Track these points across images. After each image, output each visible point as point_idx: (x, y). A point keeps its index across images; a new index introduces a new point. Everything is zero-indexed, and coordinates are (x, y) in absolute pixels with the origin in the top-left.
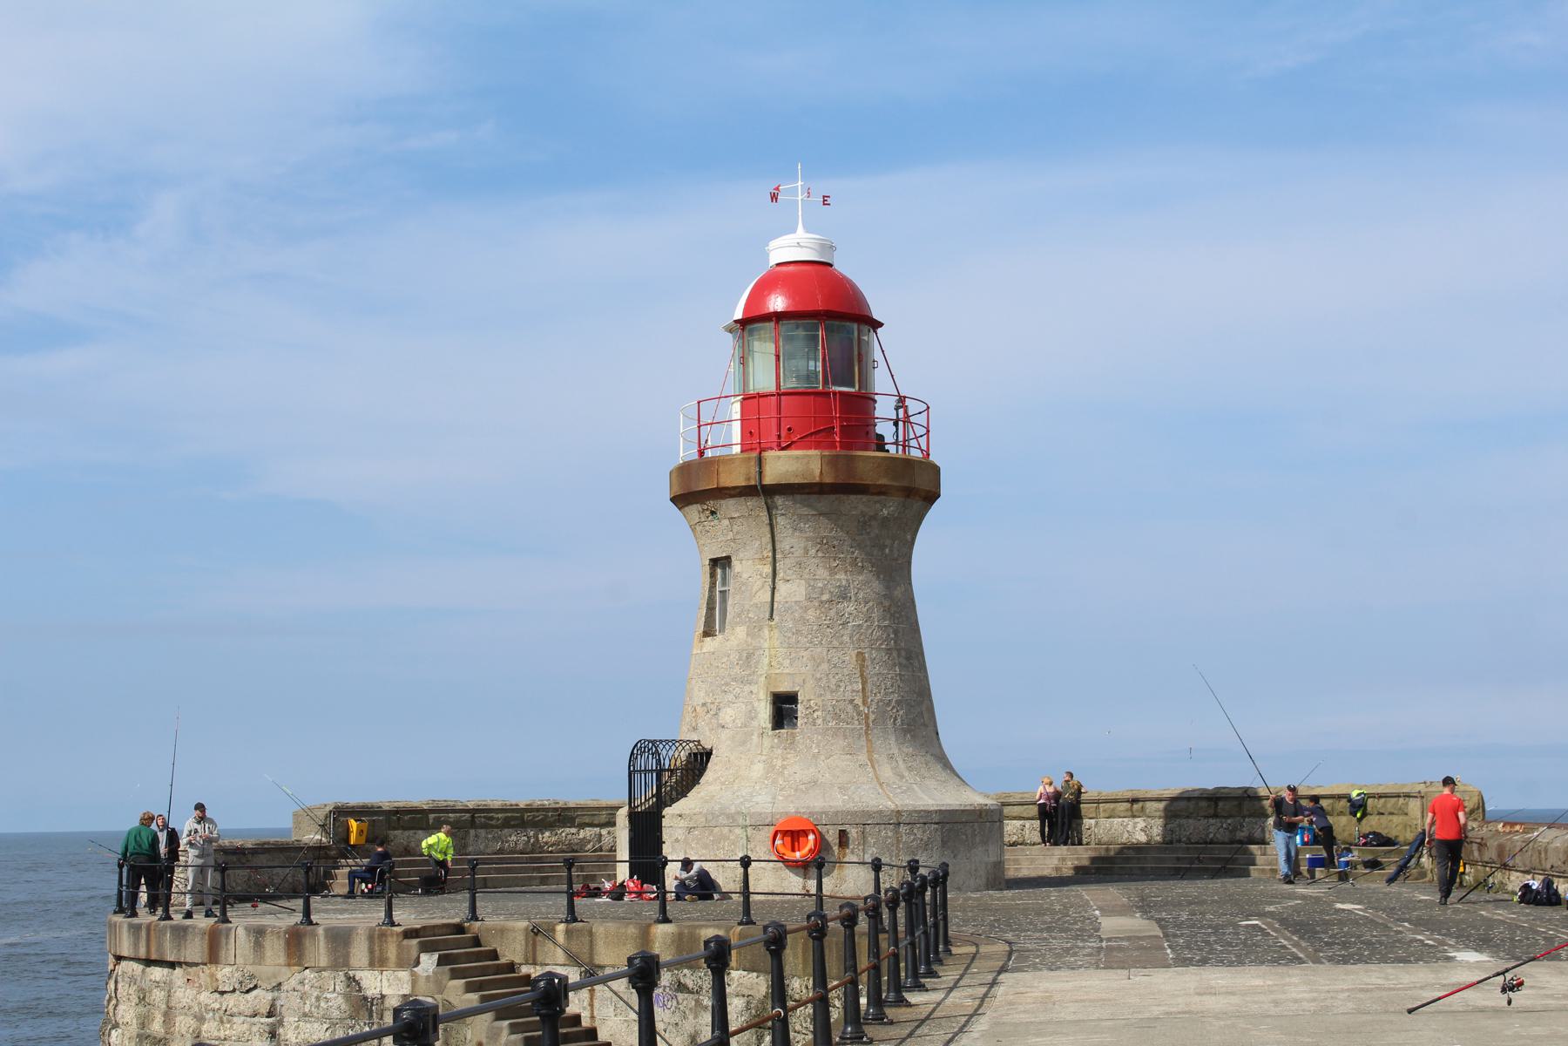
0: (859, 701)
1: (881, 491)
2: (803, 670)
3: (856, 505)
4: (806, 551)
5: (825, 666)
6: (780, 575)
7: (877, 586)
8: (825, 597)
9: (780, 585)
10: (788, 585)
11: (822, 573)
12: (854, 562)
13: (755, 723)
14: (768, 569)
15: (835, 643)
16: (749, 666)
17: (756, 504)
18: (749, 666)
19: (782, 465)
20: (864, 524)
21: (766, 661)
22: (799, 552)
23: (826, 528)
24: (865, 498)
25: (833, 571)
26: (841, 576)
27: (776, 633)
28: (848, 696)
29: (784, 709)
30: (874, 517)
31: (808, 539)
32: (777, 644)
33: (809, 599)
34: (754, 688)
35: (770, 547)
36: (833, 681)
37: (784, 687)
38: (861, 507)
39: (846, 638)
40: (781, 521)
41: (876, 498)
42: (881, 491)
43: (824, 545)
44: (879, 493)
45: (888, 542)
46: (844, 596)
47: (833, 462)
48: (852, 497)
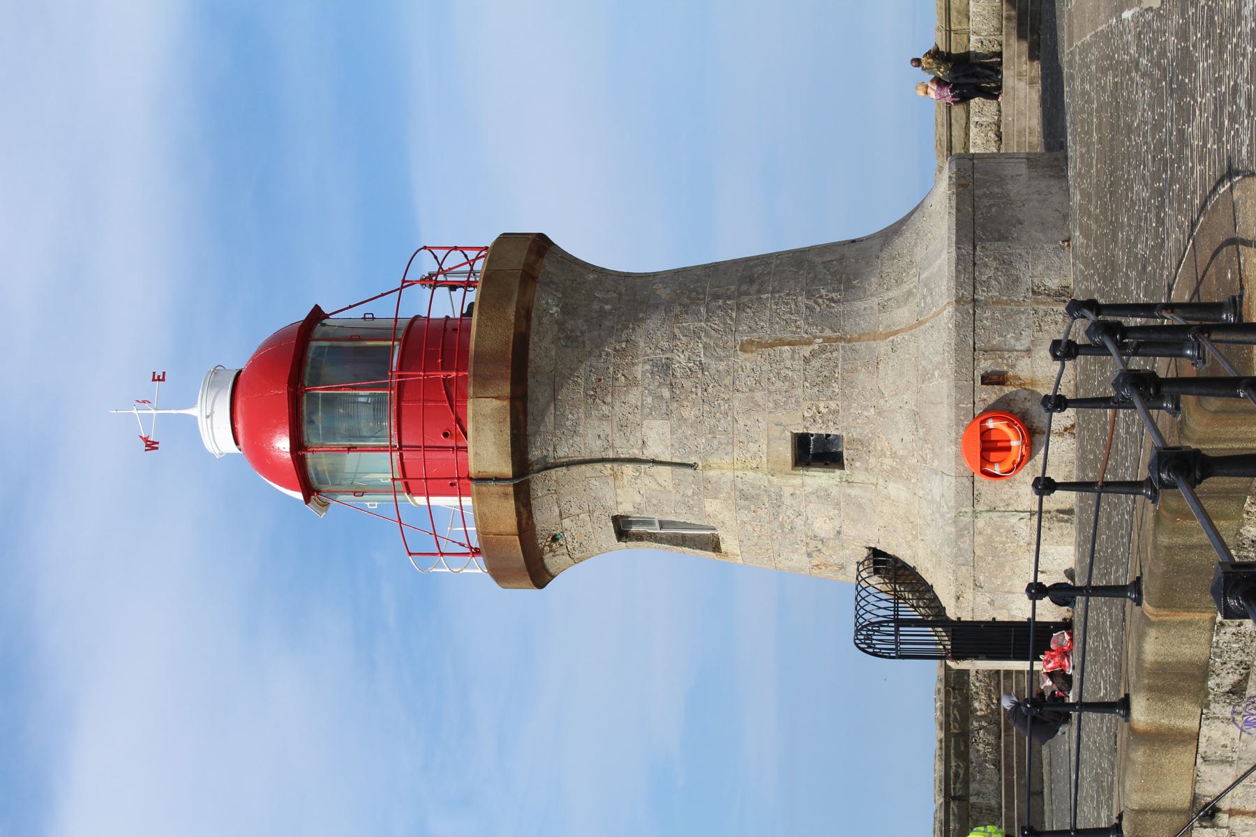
2: (763, 425)
5: (758, 395)
8: (666, 393)
10: (649, 443)
13: (835, 492)
16: (758, 497)
18: (758, 497)
21: (751, 474)
22: (606, 428)
23: (573, 392)
24: (534, 338)
29: (815, 452)
32: (728, 459)
33: (668, 415)
34: (787, 491)
36: (779, 384)
40: (564, 452)
48: (532, 355)
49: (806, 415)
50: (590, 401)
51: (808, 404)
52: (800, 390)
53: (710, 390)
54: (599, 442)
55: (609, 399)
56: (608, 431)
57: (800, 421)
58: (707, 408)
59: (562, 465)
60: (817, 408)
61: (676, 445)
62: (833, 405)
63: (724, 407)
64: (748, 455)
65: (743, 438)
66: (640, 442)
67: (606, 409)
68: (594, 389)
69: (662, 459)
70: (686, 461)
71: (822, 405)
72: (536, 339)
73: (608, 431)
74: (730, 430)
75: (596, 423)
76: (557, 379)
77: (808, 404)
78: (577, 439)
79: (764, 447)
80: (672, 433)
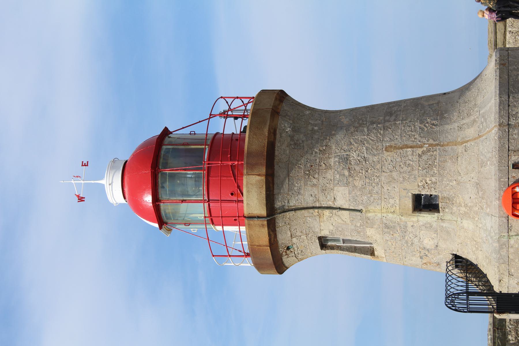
0: (420, 151)
1: (273, 132)
2: (397, 190)
3: (282, 150)
4: (314, 185)
5: (395, 174)
6: (331, 204)
7: (339, 136)
8: (346, 173)
9: (338, 204)
10: (338, 198)
11: (329, 175)
12: (323, 152)
14: (327, 212)
15: (378, 166)
17: (281, 221)
19: (253, 202)
20: (296, 145)
21: (390, 215)
22: (315, 191)
23: (298, 172)
24: (278, 144)
25: (328, 167)
26: (332, 161)
27: (371, 208)
28: (416, 158)
30: (292, 137)
31: (306, 185)
32: (378, 207)
33: (347, 184)
35: (311, 211)
37: (409, 203)
38: (283, 147)
39: (375, 159)
41: (278, 136)
42: (273, 132)
43: (311, 171)
44: (275, 134)
45: (310, 128)
46: (346, 160)
47: (251, 167)
50: (307, 177)
53: (369, 171)
54: (311, 198)
55: (316, 176)
56: (316, 192)
58: (367, 180)
59: (292, 210)
61: (352, 200)
63: (377, 180)
64: (389, 205)
65: (386, 196)
66: (333, 198)
67: (315, 181)
68: (309, 171)
69: (344, 207)
70: (357, 208)
72: (279, 145)
73: (316, 192)
74: (380, 192)
75: (310, 188)
76: (290, 165)
78: (300, 196)
79: (397, 201)
80: (349, 194)
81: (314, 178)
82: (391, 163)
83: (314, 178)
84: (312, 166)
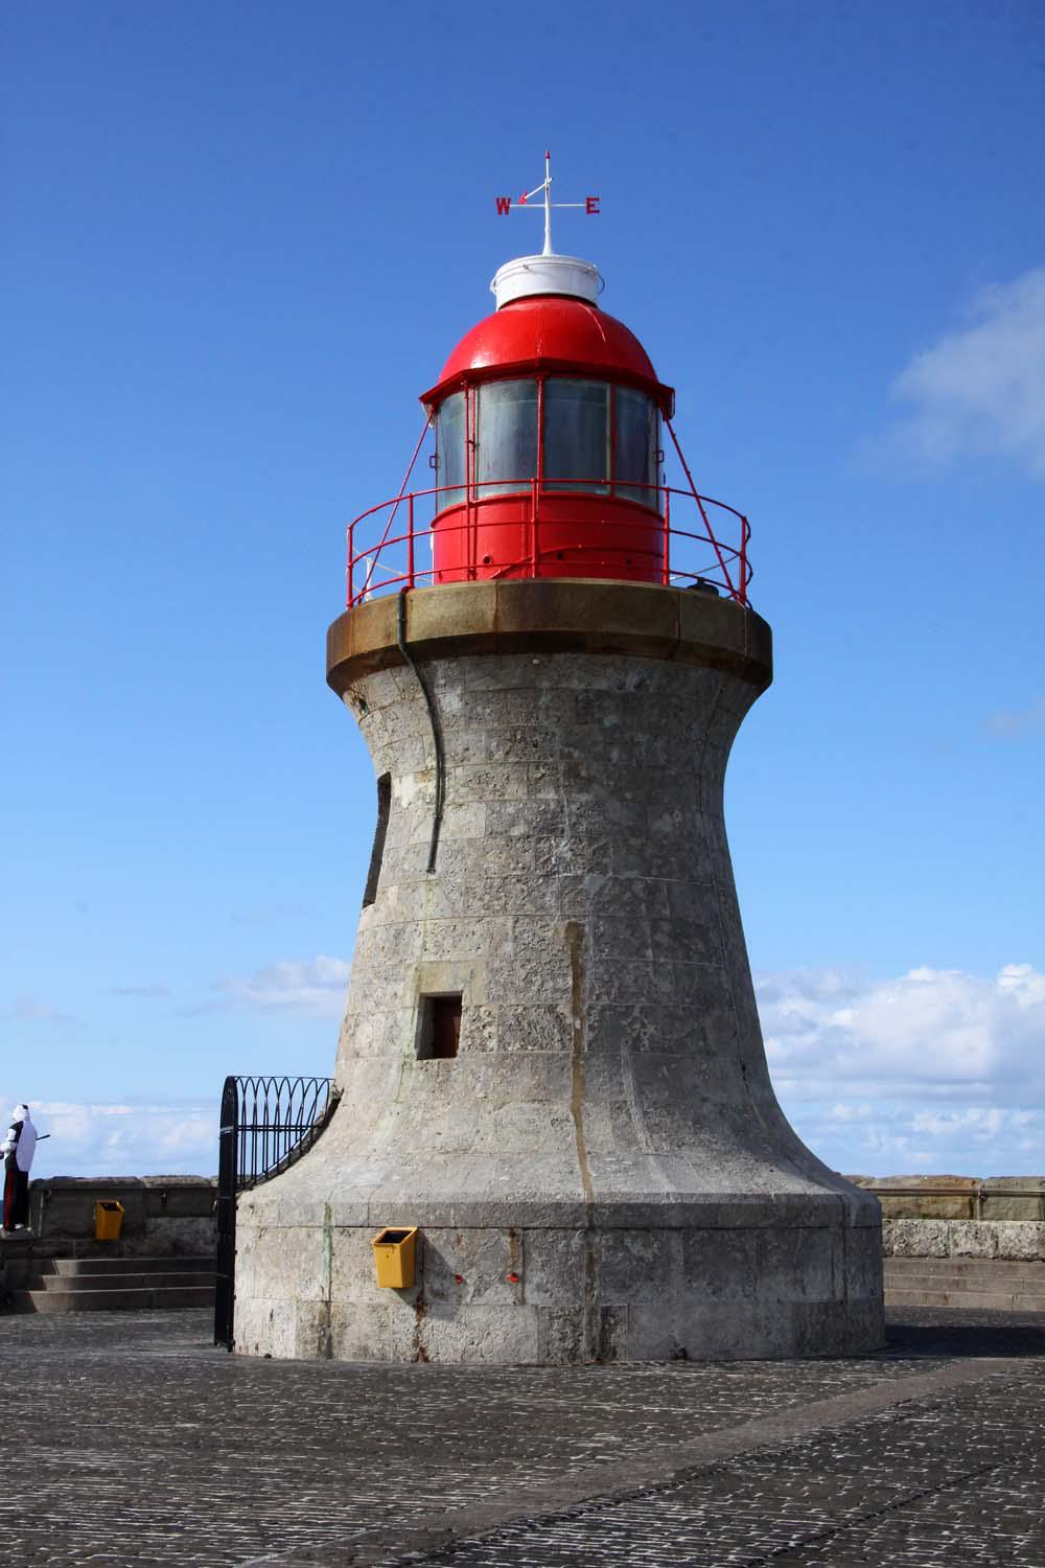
2: (472, 955)
5: (508, 948)
8: (517, 831)
29: (440, 1027)
33: (491, 834)
36: (522, 973)
37: (442, 985)
49: (482, 1009)
50: (508, 735)
51: (495, 1012)
52: (513, 1002)
53: (519, 886)
55: (512, 759)
56: (474, 760)
57: (475, 1002)
60: (490, 1024)
61: (455, 847)
62: (493, 1043)
63: (497, 905)
68: (523, 739)
71: (492, 1029)
73: (474, 760)
77: (495, 1012)
81: (507, 753)
82: (536, 939)
83: (507, 753)
84: (535, 746)
